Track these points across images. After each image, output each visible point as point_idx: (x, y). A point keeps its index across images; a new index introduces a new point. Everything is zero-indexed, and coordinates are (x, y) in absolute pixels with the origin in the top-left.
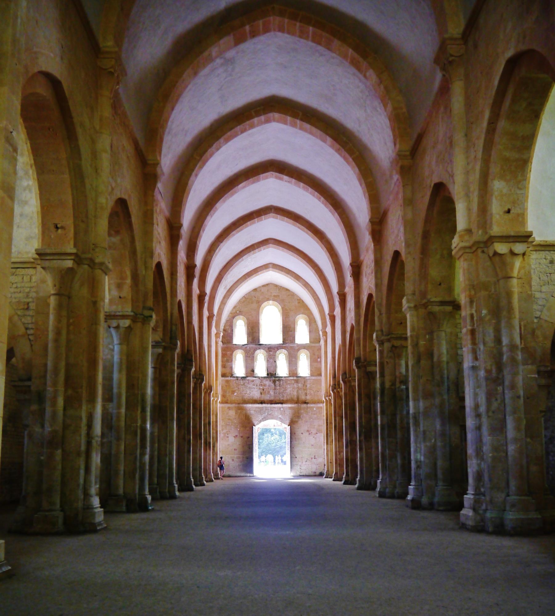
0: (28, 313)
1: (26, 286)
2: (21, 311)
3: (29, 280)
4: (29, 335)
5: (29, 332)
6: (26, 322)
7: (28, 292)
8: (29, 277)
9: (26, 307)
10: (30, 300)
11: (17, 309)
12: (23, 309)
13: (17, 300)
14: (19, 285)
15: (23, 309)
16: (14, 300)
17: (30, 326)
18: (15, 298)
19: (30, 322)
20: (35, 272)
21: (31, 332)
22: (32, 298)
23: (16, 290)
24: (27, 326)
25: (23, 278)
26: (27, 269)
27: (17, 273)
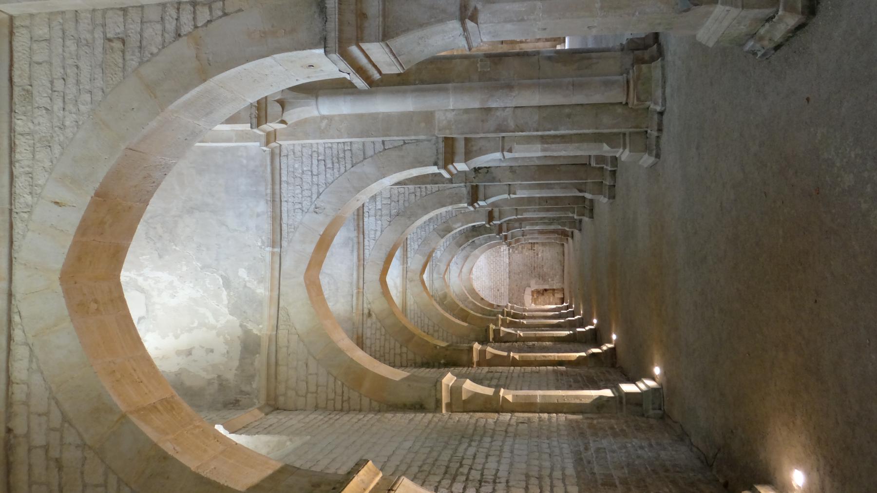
0: (133, 40)
1: (60, 50)
2: (128, 57)
3: (44, 44)
4: (196, 27)
5: (187, 28)
6: (159, 39)
7: (78, 41)
8: (35, 46)
9: (117, 45)
10: (98, 34)
11: (124, 69)
12: (123, 52)
13: (98, 71)
14: (58, 72)
15: (123, 52)
16: (99, 83)
17: (171, 26)
18: (92, 80)
19: (159, 27)
20: (24, 31)
21: (186, 17)
22: (92, 32)
23: (71, 81)
24: (169, 37)
25: (39, 63)
26: (16, 55)
27: (26, 81)
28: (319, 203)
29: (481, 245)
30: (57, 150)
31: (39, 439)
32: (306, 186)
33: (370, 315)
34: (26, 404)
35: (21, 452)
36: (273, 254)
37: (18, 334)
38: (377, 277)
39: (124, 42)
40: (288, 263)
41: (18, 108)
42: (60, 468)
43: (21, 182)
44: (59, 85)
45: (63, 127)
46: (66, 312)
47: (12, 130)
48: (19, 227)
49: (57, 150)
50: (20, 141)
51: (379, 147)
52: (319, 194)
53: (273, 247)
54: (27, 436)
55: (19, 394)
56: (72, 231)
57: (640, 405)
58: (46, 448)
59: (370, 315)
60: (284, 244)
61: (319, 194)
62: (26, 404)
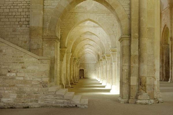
17: (115, 31)
28: (100, 34)
29: (96, 57)
30: (102, 18)
31: (72, 16)
32: (103, 32)
33: (80, 36)
34: (76, 15)
35: (71, 14)
36: (92, 26)
37: (83, 14)
38: (88, 38)
39: (113, 26)
40: (91, 28)
41: (107, 14)
42: (69, 18)
43: (99, 14)
44: (109, 18)
45: (105, 19)
46: (85, 19)
47: (105, 13)
48: (94, 14)
49: (102, 18)
50: (103, 14)
51: (109, 44)
52: (102, 34)
53: (94, 26)
54: (72, 15)
55: (77, 14)
56: (94, 20)
57: (67, 84)
58: (71, 17)
59: (80, 36)
60: (94, 28)
61: (102, 34)
62: (76, 15)
